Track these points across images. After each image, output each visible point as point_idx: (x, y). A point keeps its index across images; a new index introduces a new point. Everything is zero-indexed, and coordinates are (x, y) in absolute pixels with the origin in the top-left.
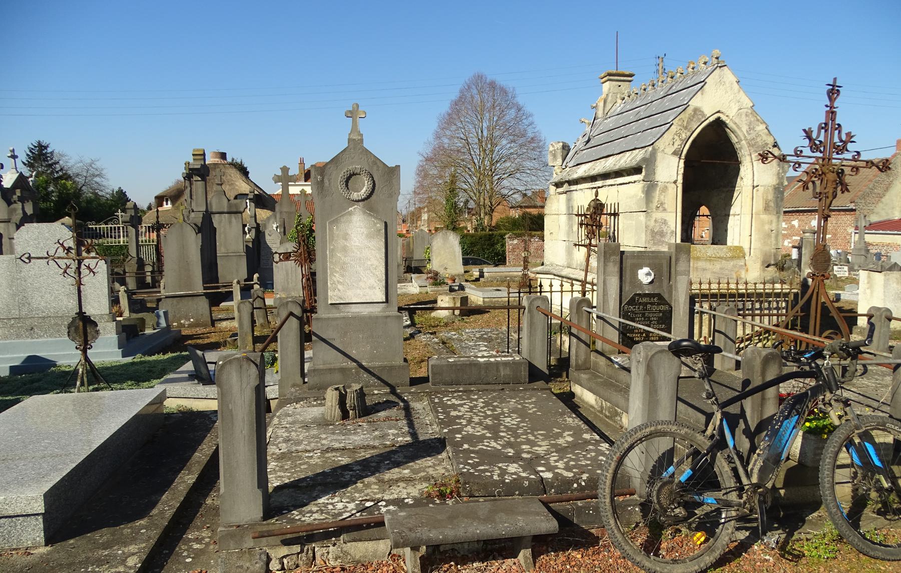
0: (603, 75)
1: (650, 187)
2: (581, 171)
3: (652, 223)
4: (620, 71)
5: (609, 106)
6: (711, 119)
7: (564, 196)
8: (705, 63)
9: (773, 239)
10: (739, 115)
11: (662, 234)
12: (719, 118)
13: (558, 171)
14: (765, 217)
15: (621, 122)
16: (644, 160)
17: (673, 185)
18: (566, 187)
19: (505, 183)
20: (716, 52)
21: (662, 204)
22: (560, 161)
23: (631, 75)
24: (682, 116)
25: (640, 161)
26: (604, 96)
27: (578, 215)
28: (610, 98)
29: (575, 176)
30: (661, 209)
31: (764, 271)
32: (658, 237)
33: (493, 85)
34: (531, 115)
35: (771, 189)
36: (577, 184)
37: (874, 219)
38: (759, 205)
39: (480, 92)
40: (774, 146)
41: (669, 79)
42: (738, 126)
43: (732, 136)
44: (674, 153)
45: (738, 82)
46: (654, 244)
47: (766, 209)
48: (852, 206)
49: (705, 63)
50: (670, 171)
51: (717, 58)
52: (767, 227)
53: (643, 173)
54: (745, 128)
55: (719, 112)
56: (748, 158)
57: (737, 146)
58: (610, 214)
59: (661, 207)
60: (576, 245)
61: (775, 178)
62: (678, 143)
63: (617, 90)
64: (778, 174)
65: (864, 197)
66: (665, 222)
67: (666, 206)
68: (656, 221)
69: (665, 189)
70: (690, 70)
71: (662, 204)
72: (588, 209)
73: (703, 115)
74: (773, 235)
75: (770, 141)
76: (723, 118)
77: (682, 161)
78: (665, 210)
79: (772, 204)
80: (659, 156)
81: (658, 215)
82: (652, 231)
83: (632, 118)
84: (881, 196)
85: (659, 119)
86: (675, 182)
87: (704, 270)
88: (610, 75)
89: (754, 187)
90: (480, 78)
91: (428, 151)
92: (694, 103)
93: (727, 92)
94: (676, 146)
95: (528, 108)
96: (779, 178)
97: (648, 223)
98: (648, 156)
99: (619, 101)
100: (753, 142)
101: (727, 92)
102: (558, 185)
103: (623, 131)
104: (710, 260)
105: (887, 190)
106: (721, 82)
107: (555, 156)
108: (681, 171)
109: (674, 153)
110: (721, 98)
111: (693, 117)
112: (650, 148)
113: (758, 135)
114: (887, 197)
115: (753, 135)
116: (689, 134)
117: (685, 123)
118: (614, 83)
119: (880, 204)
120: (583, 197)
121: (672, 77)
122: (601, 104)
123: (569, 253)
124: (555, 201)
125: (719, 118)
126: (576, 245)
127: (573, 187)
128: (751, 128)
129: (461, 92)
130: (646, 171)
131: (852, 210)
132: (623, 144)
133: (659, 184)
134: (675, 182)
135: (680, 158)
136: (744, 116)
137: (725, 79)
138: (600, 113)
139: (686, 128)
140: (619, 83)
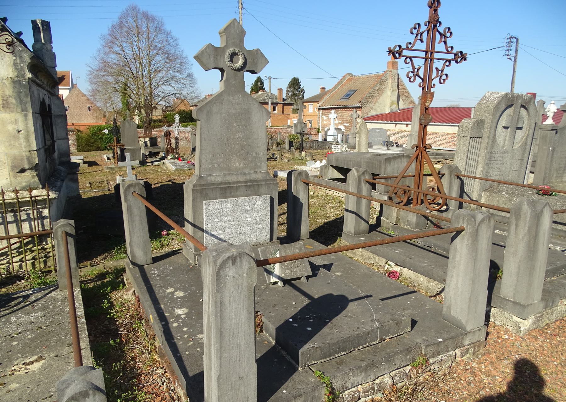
9: (22, 141)
19: (160, 89)
31: (15, 177)
33: (146, 16)
34: (177, 39)
37: (373, 113)
39: (136, 20)
48: (360, 105)
64: (15, 64)
65: (367, 98)
84: (377, 98)
90: (134, 8)
91: (96, 65)
95: (174, 34)
96: (17, 69)
105: (381, 94)
114: (381, 99)
119: (377, 104)
129: (120, 19)
131: (361, 107)
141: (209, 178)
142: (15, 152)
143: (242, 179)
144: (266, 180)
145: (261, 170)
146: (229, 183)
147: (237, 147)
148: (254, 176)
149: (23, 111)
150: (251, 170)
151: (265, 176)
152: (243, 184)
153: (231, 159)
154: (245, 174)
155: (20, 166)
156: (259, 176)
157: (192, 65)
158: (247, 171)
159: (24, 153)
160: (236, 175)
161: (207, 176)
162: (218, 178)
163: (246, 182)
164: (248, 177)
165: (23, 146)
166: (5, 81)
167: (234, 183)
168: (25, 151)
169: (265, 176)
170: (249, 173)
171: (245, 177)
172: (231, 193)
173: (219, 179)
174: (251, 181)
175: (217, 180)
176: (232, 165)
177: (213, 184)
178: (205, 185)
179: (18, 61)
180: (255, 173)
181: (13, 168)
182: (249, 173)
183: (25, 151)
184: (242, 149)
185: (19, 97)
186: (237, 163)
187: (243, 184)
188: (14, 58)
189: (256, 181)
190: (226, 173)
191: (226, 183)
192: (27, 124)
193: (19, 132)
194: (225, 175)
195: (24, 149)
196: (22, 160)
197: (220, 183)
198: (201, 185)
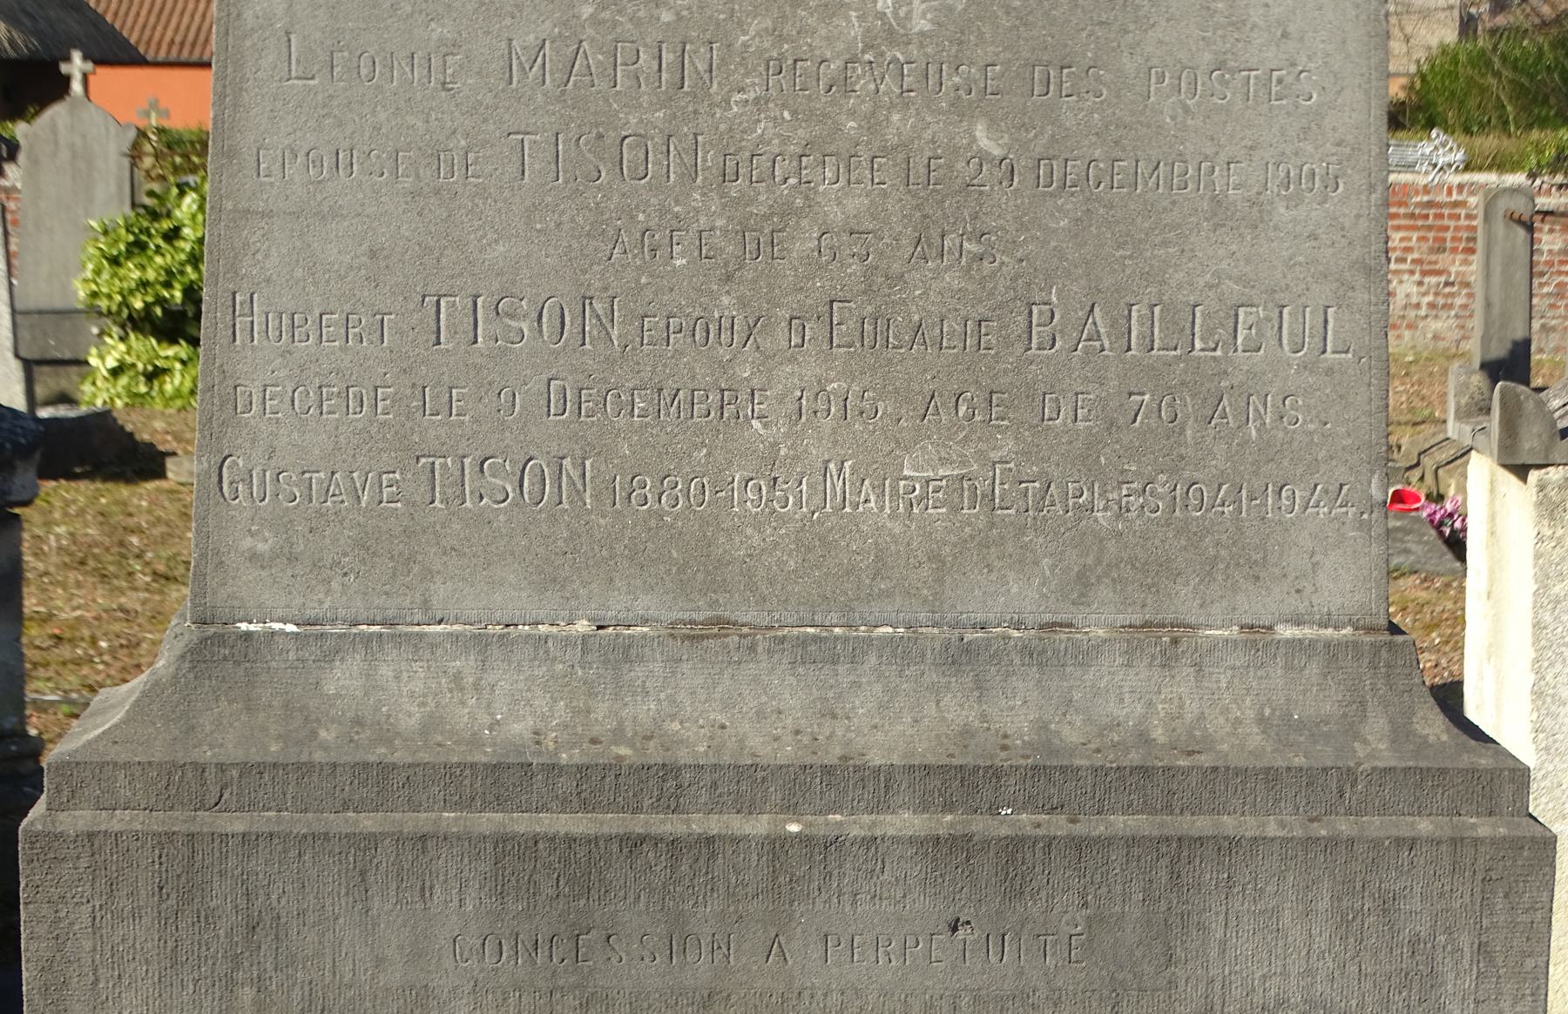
141: (343, 677)
143: (892, 721)
144: (1333, 785)
145: (1258, 605)
146: (665, 781)
147: (840, 200)
148: (1123, 702)
150: (1083, 582)
151: (1319, 699)
152: (905, 822)
153: (730, 402)
154: (962, 657)
156: (1218, 706)
158: (1011, 597)
160: (813, 653)
161: (319, 642)
162: (503, 680)
163: (957, 781)
164: (1016, 713)
167: (745, 783)
169: (1319, 699)
170: (1049, 646)
171: (957, 709)
172: (678, 942)
173: (514, 710)
174: (1046, 777)
175: (465, 714)
176: (749, 502)
177: (381, 781)
178: (290, 777)
180: (1161, 639)
182: (1049, 646)
184: (925, 244)
186: (833, 468)
187: (905, 822)
189: (1143, 779)
190: (647, 607)
191: (593, 783)
194: (627, 653)
197: (508, 778)
198: (186, 783)
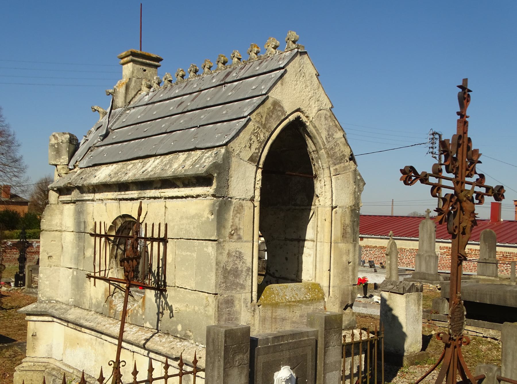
0: (123, 54)
1: (223, 204)
2: (103, 174)
3: (224, 258)
4: (144, 52)
5: (132, 93)
6: (292, 118)
7: (71, 207)
8: (275, 48)
10: (319, 117)
11: (236, 273)
12: (299, 117)
13: (63, 172)
14: (343, 246)
15: (155, 114)
16: (215, 166)
17: (250, 204)
18: (75, 195)
20: (293, 35)
21: (236, 230)
22: (65, 158)
23: (159, 60)
24: (260, 110)
25: (210, 167)
26: (125, 80)
27: (94, 235)
28: (133, 84)
29: (94, 181)
30: (235, 237)
32: (231, 278)
35: (348, 211)
36: (94, 192)
38: (337, 231)
40: (351, 159)
41: (220, 65)
42: (317, 130)
43: (309, 142)
44: (252, 159)
45: (318, 76)
46: (227, 288)
47: (344, 235)
49: (275, 48)
50: (246, 182)
51: (294, 42)
52: (344, 259)
53: (214, 186)
54: (324, 134)
55: (298, 110)
56: (327, 171)
57: (314, 155)
58: (152, 239)
59: (235, 234)
60: (89, 276)
61: (352, 197)
62: (255, 145)
63: (141, 74)
64: (355, 192)
66: (240, 256)
67: (241, 233)
68: (229, 254)
69: (240, 209)
70: (253, 54)
71: (236, 230)
72: (111, 228)
73: (284, 112)
74: (350, 268)
75: (347, 152)
76: (304, 119)
77: (260, 171)
78: (240, 238)
79: (349, 230)
80: (234, 161)
81: (231, 246)
82: (225, 269)
83: (172, 109)
85: (227, 112)
86: (252, 199)
87: (283, 319)
88: (133, 54)
89: (333, 208)
92: (274, 95)
93: (306, 86)
94: (253, 150)
96: (355, 198)
97: (220, 258)
98: (220, 161)
99: (145, 90)
100: (332, 152)
101: (306, 86)
102: (62, 191)
103: (164, 125)
104: (290, 306)
106: (300, 72)
107: (58, 152)
108: (259, 185)
109: (252, 159)
110: (300, 93)
111: (272, 112)
112: (223, 150)
113: (337, 145)
115: (332, 144)
116: (267, 134)
117: (263, 120)
118: (138, 66)
120: (104, 211)
121: (224, 63)
122: (122, 90)
123: (78, 286)
124: (57, 212)
125: (299, 117)
126: (89, 276)
127: (87, 196)
128: (330, 135)
130: (218, 182)
132: (191, 138)
133: (234, 201)
134: (252, 199)
135: (258, 168)
136: (323, 119)
137: (305, 70)
138: (120, 101)
139: (264, 126)
140: (145, 68)
142: (345, 285)
149: (354, 241)
155: (346, 302)
157: (19, 145)
159: (350, 287)
165: (350, 279)
166: (346, 209)
168: (350, 285)
179: (357, 190)
181: (342, 303)
183: (350, 285)
185: (353, 225)
188: (355, 187)
192: (354, 255)
193: (349, 263)
195: (350, 283)
196: (348, 295)
